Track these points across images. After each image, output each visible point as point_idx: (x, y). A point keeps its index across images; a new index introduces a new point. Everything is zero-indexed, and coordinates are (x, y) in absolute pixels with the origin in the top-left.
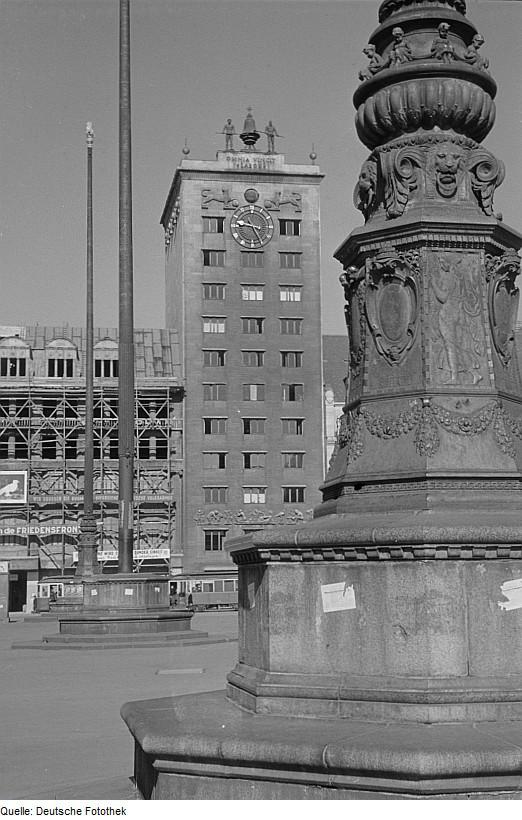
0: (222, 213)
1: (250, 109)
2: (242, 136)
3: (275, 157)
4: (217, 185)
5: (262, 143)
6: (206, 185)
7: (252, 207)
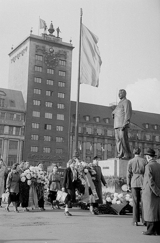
0: (42, 54)
1: (52, 22)
3: (59, 39)
4: (41, 45)
5: (55, 34)
6: (37, 44)
7: (52, 54)
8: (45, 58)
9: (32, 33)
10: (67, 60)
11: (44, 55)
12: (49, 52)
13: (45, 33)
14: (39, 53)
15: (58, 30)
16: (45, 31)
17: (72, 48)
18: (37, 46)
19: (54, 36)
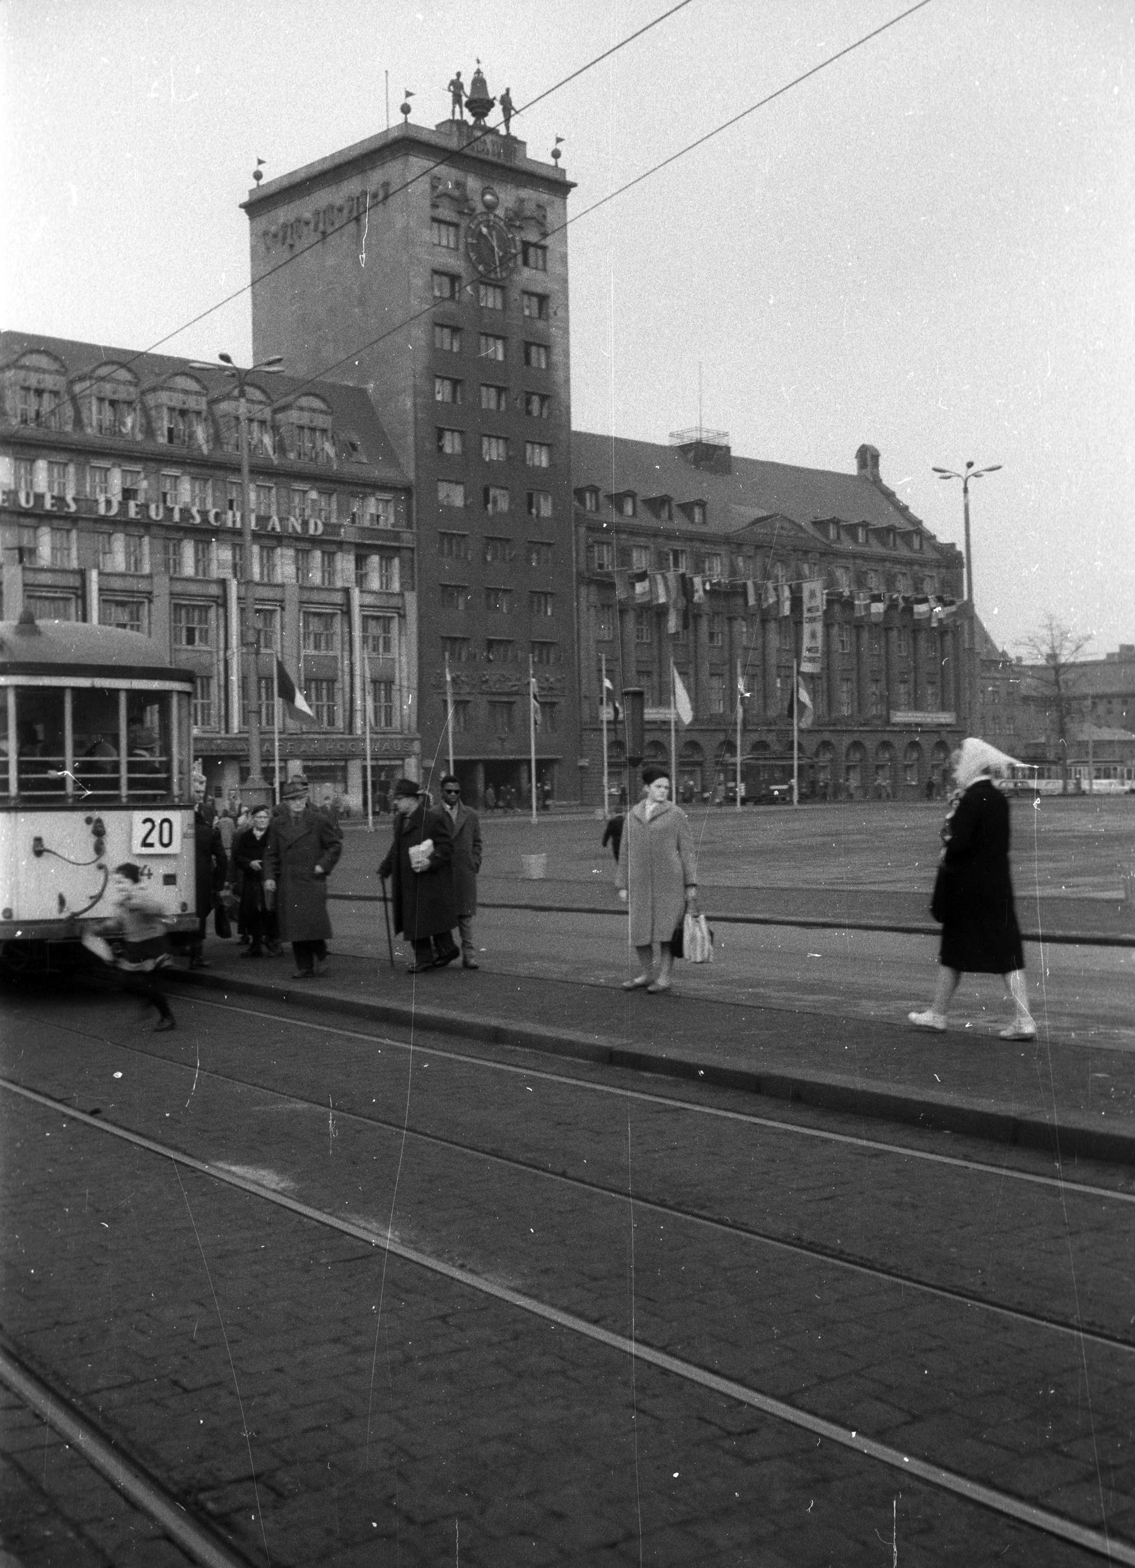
2: (468, 105)
4: (449, 175)
7: (492, 217)
9: (412, 119)
10: (548, 242)
11: (464, 223)
13: (457, 117)
15: (506, 102)
16: (457, 108)
18: (435, 182)
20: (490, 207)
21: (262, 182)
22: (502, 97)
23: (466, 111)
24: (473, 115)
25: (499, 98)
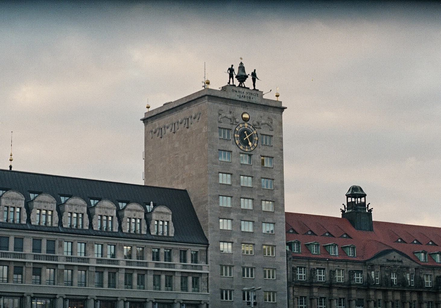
0: (229, 126)
1: (241, 59)
2: (236, 77)
8: (236, 132)
9: (210, 87)
12: (242, 121)
14: (223, 125)
15: (254, 74)
17: (282, 109)
19: (248, 88)
20: (246, 120)
21: (150, 109)
22: (252, 73)
23: (236, 80)
24: (239, 81)
25: (251, 74)
